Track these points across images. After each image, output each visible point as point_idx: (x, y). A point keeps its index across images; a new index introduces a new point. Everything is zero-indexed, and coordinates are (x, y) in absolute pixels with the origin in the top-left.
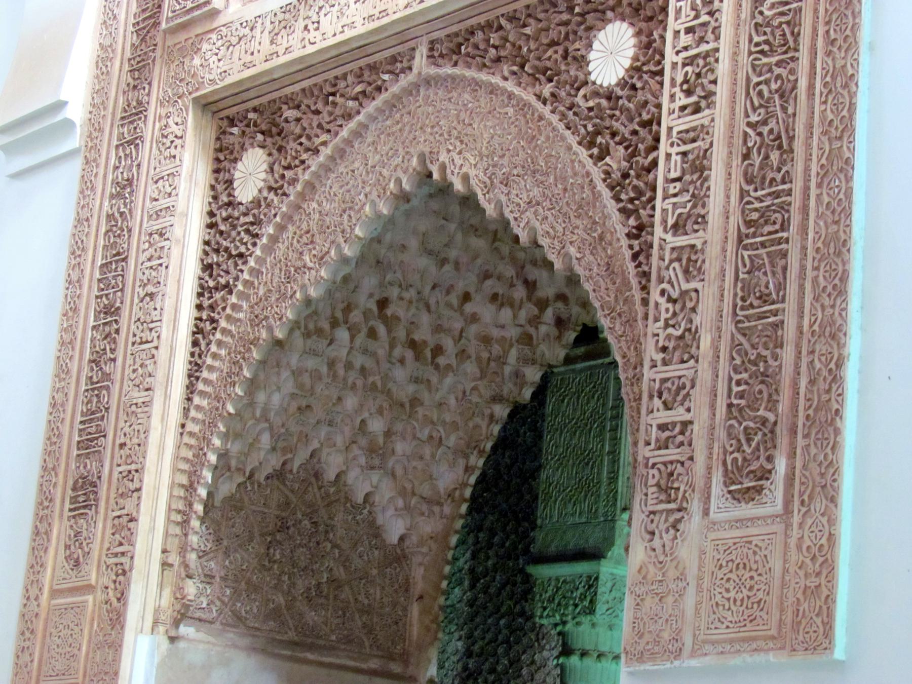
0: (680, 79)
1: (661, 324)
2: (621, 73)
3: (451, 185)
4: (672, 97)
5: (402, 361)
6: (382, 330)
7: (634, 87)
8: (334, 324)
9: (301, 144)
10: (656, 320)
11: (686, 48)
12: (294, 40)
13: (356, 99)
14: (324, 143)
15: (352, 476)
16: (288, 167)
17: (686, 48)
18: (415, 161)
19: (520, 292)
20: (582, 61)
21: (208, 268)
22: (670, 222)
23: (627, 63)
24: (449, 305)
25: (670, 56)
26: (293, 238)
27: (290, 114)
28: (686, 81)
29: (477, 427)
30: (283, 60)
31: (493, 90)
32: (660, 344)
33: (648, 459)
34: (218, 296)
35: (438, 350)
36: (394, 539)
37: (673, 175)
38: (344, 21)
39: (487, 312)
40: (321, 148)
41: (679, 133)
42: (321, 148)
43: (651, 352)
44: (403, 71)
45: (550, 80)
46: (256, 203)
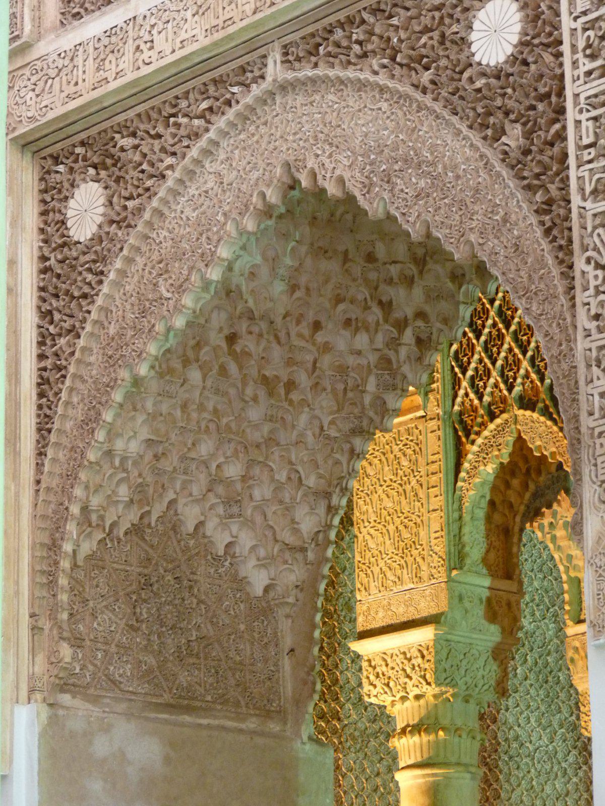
0: (581, 44)
1: (592, 291)
2: (509, 50)
3: (323, 191)
4: (575, 63)
5: (255, 399)
6: (233, 368)
7: (525, 63)
8: (186, 362)
9: (143, 171)
10: (586, 289)
11: (585, 13)
12: (126, 62)
13: (202, 116)
14: (171, 167)
15: (210, 528)
16: (130, 198)
17: (585, 13)
18: (278, 171)
19: (377, 312)
20: (463, 43)
21: (46, 315)
22: (588, 189)
23: (515, 39)
24: (300, 336)
25: (566, 23)
26: (144, 270)
27: (127, 142)
28: (589, 46)
29: (337, 462)
30: (113, 85)
31: (362, 86)
32: (593, 312)
33: (593, 429)
34: (62, 341)
35: (291, 385)
36: (259, 592)
37: (586, 141)
38: (183, 35)
39: (341, 341)
40: (169, 173)
41: (588, 98)
42: (169, 173)
43: (583, 320)
44: (255, 80)
45: (427, 68)
46: (98, 239)
